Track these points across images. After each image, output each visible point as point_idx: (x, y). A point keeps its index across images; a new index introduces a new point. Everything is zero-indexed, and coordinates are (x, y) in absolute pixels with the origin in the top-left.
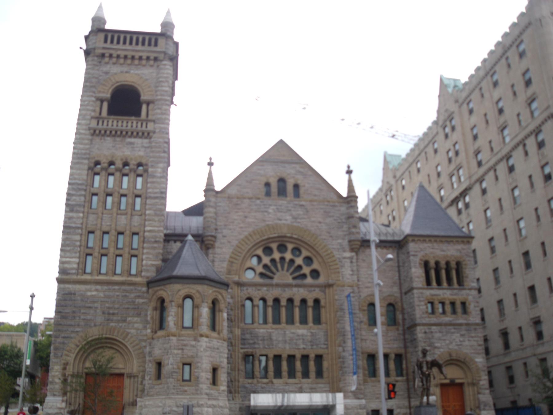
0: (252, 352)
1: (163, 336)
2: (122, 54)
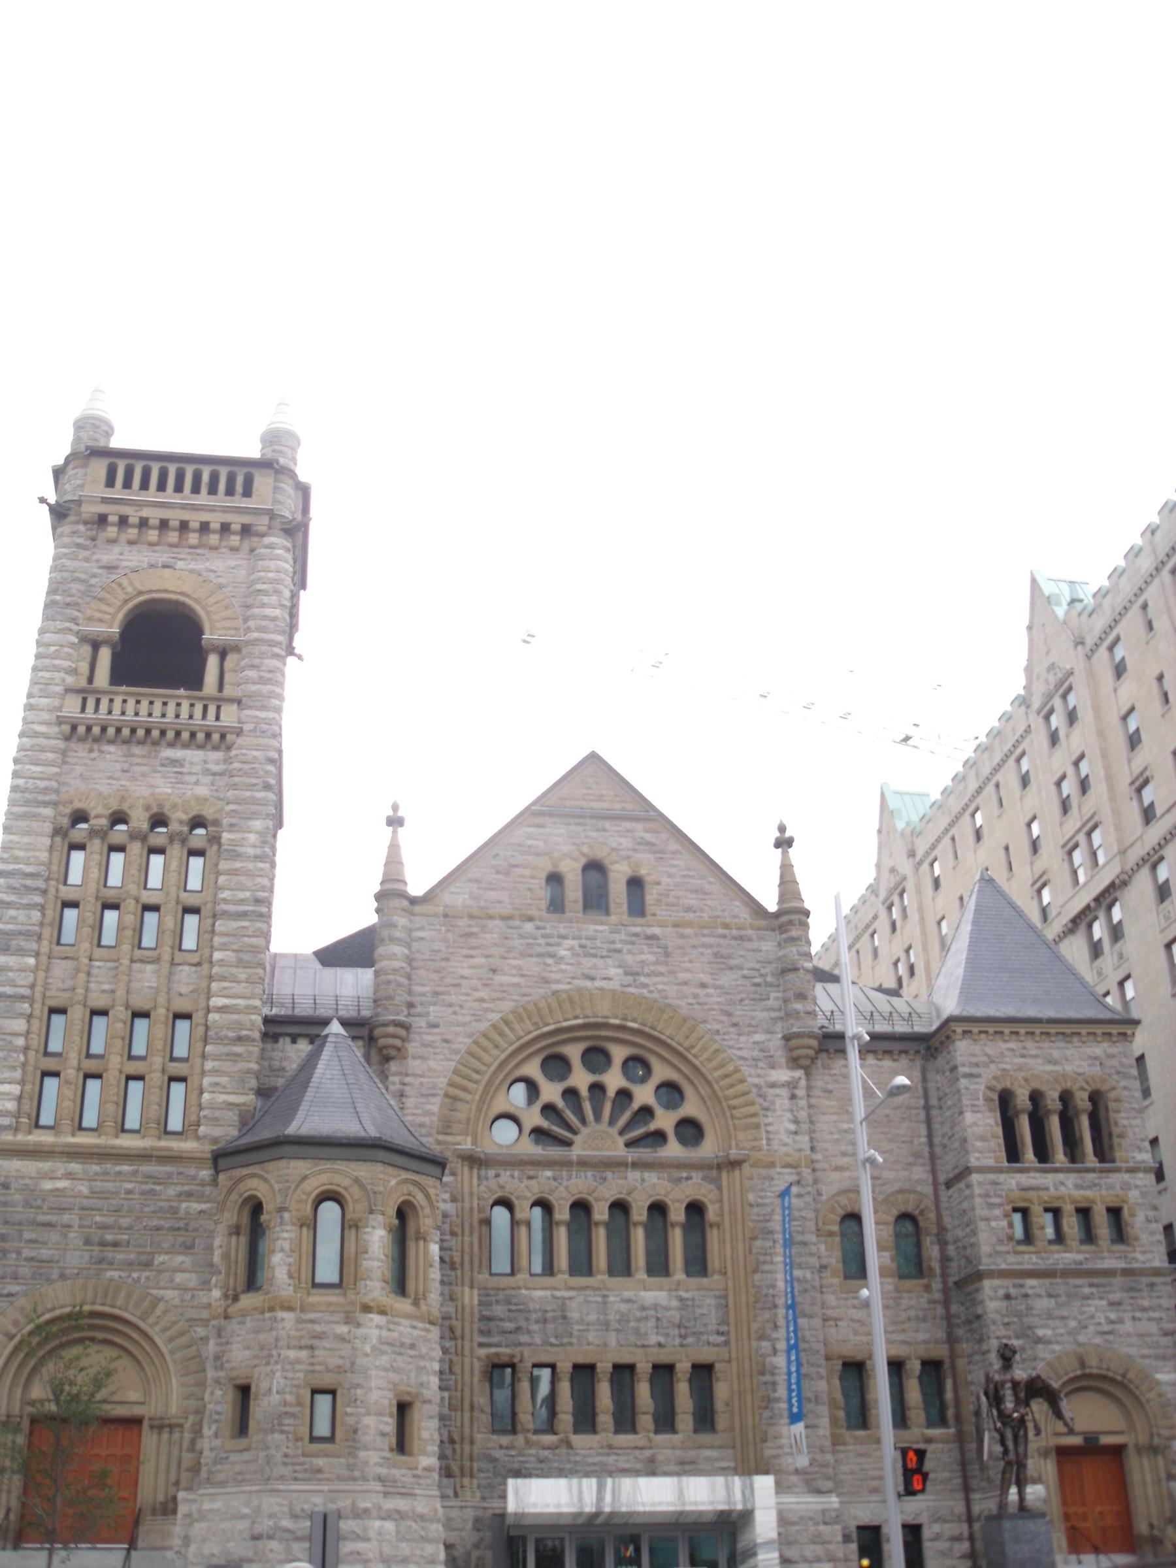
0: (512, 1356)
1: (255, 1309)
2: (154, 515)
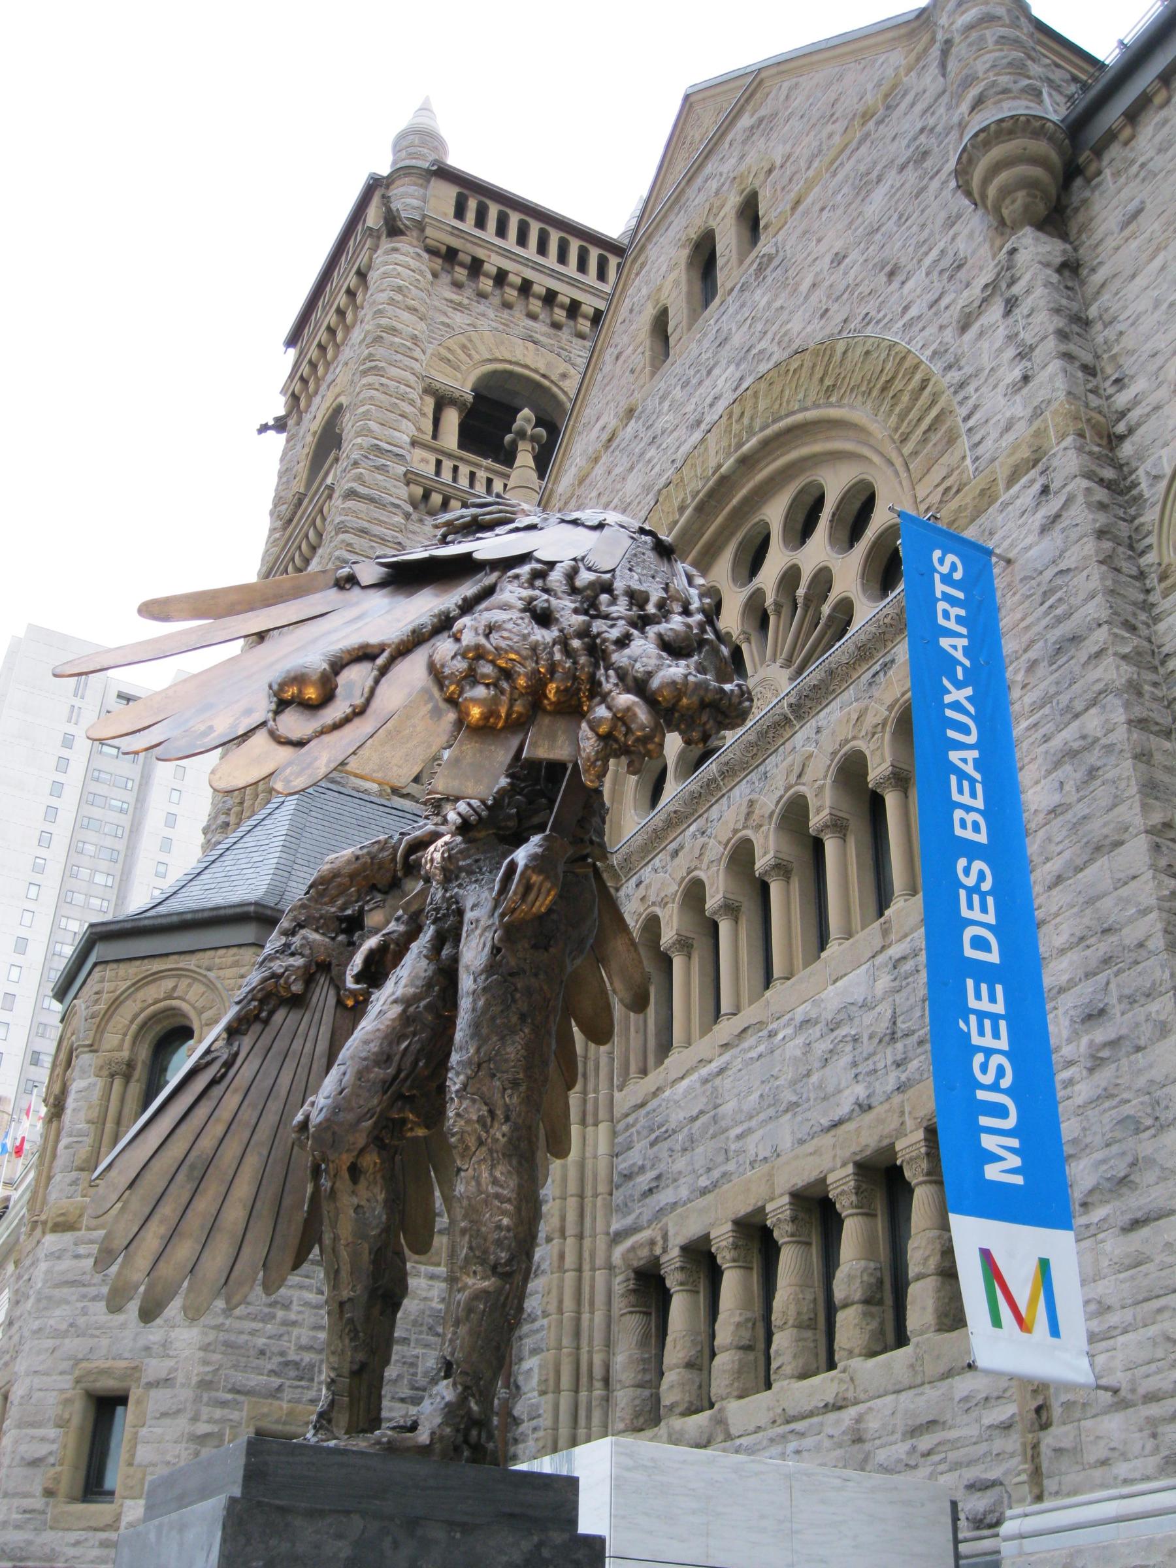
0: (652, 1243)
